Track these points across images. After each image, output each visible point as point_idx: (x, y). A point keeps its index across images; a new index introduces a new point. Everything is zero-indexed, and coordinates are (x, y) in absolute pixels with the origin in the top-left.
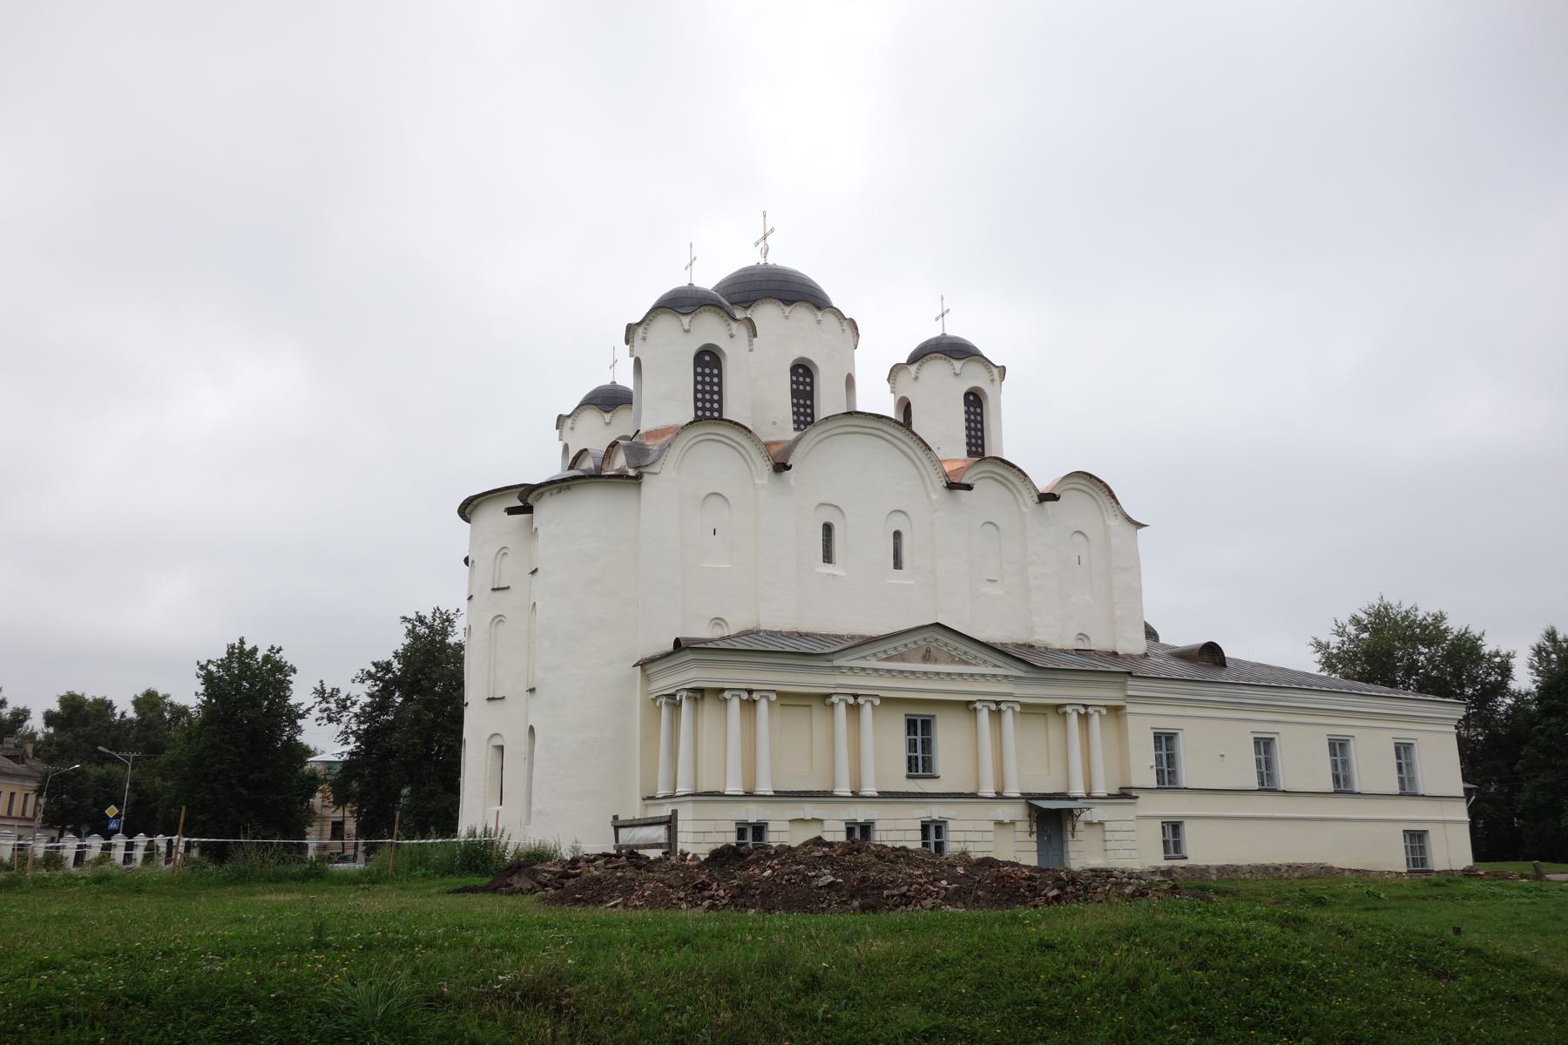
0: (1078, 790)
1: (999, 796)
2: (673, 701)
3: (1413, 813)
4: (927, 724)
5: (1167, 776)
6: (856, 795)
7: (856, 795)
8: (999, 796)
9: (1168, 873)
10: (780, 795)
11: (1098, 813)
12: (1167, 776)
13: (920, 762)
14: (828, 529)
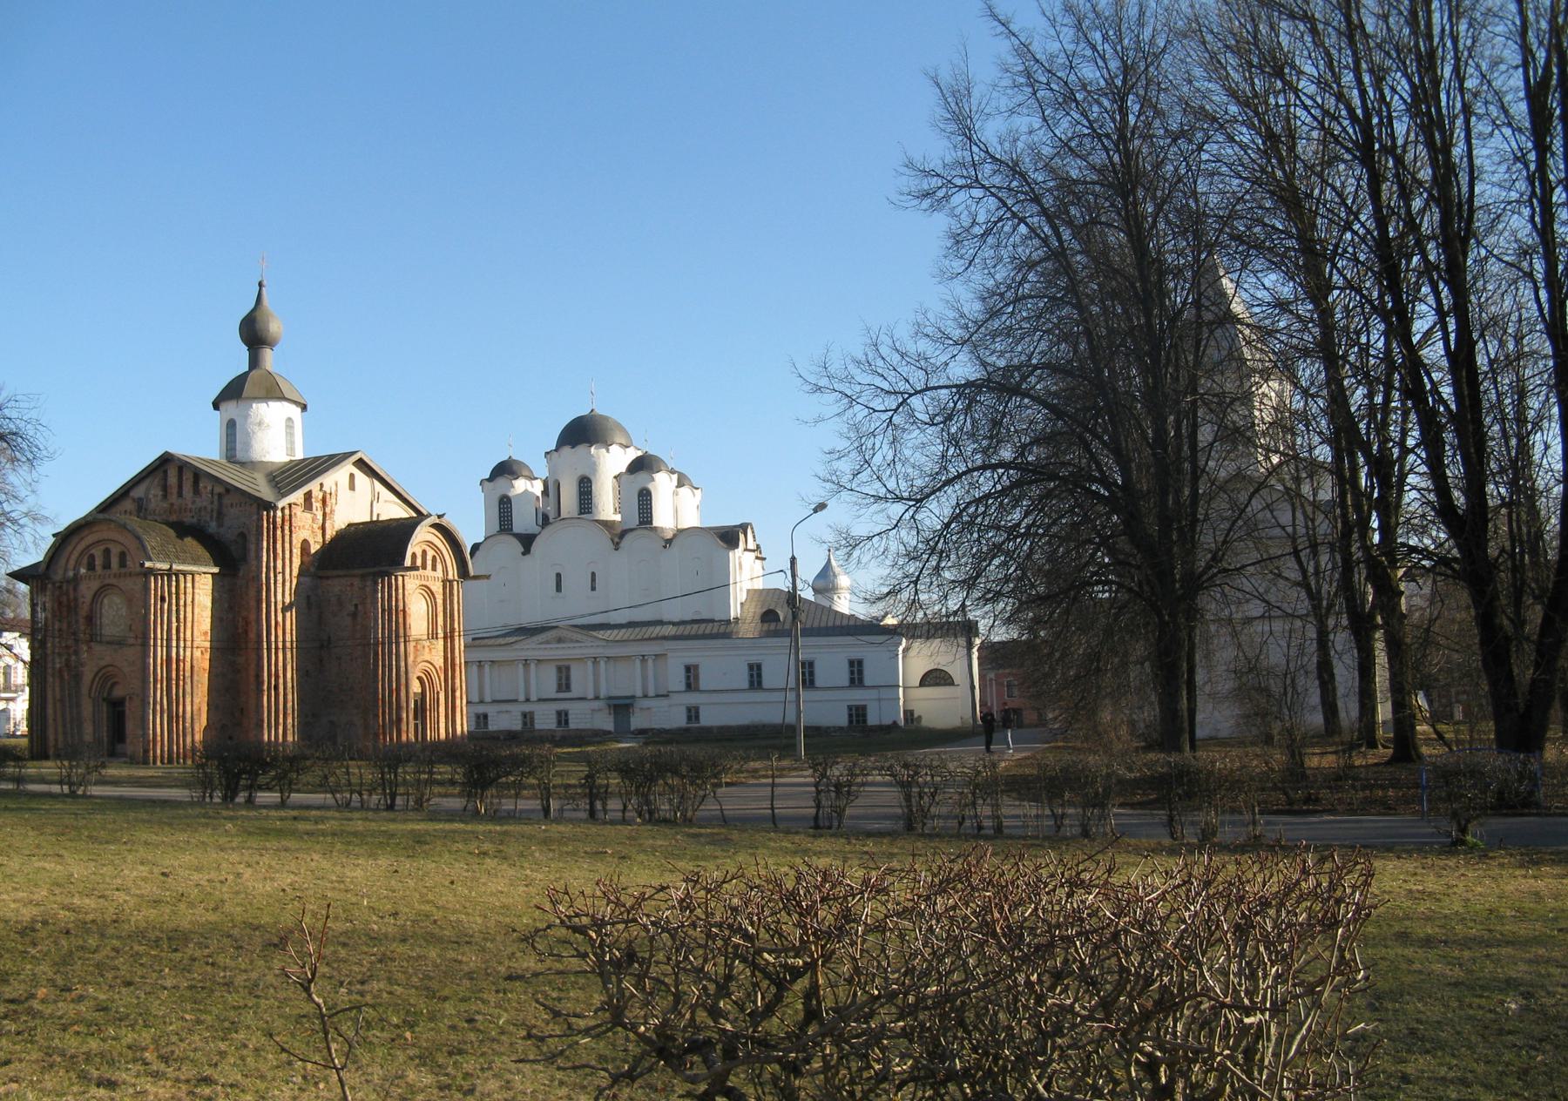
0: (639, 693)
1: (597, 698)
2: (480, 664)
3: (857, 696)
4: (568, 668)
5: (691, 683)
6: (528, 700)
7: (528, 700)
8: (597, 698)
9: (687, 730)
10: (494, 701)
11: (646, 703)
12: (691, 683)
13: (564, 684)
14: (559, 576)
